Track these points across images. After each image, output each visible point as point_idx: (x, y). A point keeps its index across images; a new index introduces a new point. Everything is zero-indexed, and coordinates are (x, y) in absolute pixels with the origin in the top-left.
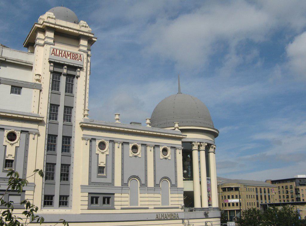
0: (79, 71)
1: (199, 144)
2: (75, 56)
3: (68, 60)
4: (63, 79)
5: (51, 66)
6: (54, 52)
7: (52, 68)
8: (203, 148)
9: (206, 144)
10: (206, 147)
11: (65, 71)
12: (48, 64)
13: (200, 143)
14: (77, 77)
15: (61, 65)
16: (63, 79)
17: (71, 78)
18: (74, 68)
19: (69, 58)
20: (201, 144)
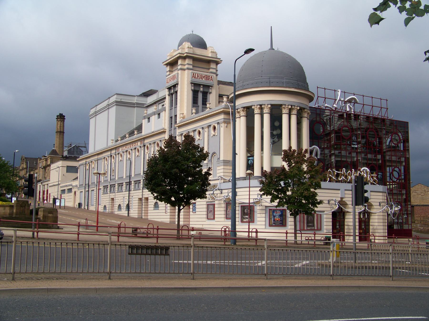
0: (211, 89)
1: (290, 107)
2: (207, 78)
3: (203, 81)
4: (200, 96)
5: (192, 86)
6: (194, 76)
7: (193, 88)
8: (294, 112)
9: (298, 108)
10: (298, 111)
11: (202, 89)
12: (190, 85)
13: (292, 106)
14: (210, 93)
15: (199, 85)
16: (200, 96)
17: (205, 95)
18: (208, 87)
19: (204, 79)
20: (293, 107)
